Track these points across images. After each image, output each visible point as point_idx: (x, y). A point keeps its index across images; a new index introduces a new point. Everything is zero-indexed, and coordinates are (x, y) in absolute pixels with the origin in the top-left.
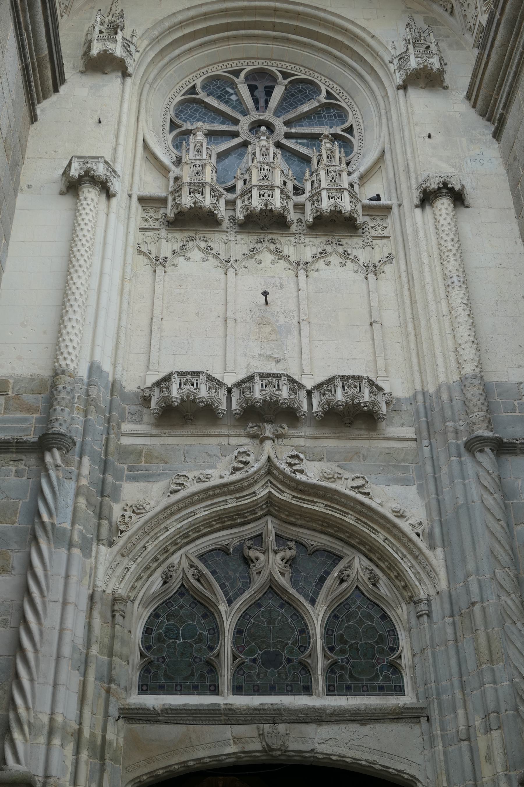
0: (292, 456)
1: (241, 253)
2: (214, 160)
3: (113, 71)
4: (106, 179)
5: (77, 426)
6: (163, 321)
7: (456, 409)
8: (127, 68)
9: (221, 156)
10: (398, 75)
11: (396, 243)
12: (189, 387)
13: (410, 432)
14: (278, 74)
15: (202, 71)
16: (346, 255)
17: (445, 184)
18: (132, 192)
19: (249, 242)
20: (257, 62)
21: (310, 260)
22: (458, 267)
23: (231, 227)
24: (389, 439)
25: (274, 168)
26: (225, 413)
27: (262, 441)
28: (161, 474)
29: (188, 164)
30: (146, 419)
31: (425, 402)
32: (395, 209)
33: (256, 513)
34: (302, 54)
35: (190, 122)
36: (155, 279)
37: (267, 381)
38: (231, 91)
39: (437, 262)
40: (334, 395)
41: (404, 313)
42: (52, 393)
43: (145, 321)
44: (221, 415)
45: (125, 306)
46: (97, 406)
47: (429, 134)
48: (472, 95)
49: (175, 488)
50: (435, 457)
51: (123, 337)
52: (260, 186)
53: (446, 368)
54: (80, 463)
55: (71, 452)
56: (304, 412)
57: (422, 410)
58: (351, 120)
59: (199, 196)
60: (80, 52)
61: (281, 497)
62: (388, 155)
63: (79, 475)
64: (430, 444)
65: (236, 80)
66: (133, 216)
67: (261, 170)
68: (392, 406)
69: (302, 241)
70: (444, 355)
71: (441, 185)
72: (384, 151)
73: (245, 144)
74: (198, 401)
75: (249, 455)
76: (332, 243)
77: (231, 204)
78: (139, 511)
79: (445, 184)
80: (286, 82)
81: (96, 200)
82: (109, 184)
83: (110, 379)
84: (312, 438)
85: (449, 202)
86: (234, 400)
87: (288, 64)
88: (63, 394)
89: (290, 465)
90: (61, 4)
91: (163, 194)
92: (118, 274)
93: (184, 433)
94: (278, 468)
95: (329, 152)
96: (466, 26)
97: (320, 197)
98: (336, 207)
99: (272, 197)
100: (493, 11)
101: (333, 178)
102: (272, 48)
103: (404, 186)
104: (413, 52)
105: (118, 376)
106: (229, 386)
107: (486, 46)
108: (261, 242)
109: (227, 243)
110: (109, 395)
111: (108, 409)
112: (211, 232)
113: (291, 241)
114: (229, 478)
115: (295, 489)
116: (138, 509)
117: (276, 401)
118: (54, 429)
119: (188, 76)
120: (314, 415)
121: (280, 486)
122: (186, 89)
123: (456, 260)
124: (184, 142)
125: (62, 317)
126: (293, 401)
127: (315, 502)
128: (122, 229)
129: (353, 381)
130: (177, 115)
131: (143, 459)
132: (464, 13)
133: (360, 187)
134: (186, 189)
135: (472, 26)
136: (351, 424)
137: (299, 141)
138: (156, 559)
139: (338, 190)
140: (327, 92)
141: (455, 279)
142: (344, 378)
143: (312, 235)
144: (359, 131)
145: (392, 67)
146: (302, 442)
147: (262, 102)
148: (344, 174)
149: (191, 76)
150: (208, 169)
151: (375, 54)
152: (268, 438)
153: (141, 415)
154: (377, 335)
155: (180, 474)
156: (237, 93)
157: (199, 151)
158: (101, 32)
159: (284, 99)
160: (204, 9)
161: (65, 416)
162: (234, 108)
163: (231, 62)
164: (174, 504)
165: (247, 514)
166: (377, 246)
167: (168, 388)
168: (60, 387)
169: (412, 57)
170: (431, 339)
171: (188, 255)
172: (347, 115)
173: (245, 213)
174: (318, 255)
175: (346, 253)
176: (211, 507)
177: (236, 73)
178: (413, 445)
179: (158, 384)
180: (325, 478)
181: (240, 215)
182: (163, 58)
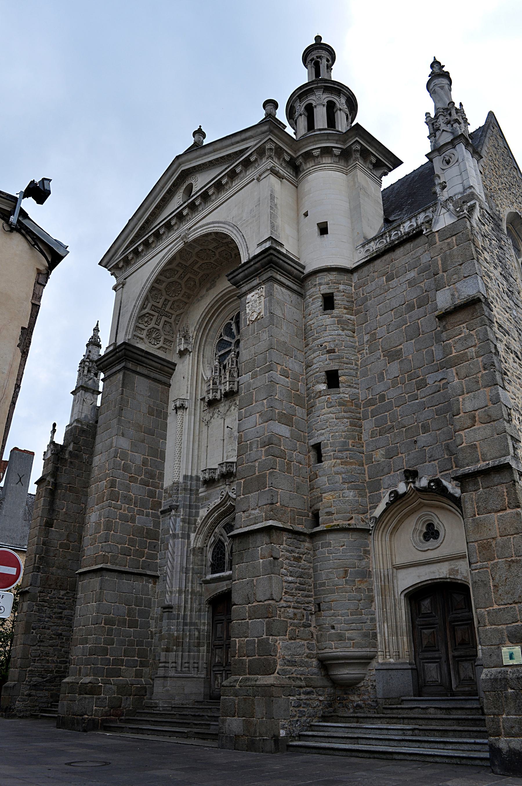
138: (209, 533)
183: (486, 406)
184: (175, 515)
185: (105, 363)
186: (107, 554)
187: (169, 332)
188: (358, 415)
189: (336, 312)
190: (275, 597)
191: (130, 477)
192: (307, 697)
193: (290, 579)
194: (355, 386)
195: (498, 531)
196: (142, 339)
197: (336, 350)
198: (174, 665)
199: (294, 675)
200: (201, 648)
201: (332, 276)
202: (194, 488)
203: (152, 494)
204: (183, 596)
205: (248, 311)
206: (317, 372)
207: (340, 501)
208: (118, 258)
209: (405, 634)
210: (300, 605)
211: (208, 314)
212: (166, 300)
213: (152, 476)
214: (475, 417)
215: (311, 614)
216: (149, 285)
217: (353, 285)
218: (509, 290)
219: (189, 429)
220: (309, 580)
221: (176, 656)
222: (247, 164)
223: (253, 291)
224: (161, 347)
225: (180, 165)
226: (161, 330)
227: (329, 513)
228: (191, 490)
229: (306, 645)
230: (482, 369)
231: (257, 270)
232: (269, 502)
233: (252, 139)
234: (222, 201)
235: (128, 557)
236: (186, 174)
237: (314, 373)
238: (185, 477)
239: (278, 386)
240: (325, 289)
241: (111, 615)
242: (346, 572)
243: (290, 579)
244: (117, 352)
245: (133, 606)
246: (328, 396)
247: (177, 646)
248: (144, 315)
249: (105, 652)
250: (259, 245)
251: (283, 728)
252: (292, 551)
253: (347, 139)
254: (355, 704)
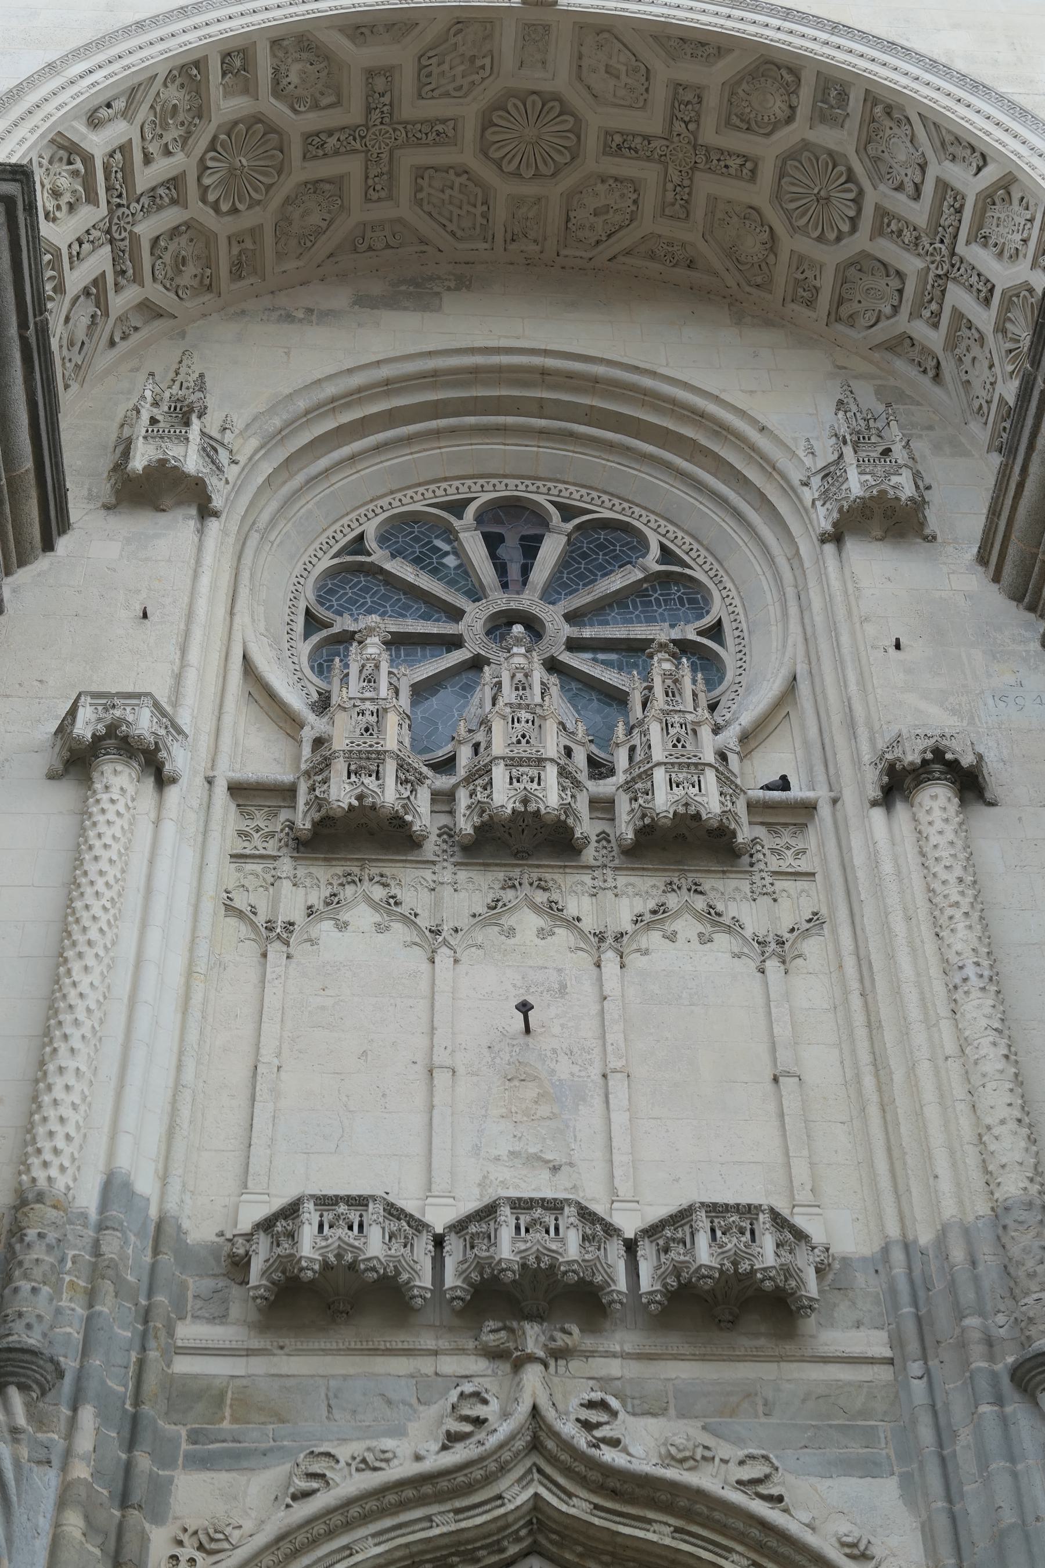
0: (591, 1405)
1: (466, 913)
2: (405, 700)
3: (179, 503)
4: (156, 743)
5: (68, 1330)
6: (282, 1073)
7: (986, 1284)
8: (209, 499)
9: (422, 691)
10: (822, 511)
11: (829, 887)
12: (342, 1232)
13: (876, 1344)
14: (551, 508)
15: (380, 503)
16: (712, 915)
17: (938, 753)
18: (215, 773)
19: (484, 887)
20: (503, 484)
21: (629, 927)
22: (975, 943)
23: (445, 851)
24: (826, 1360)
25: (544, 718)
26: (428, 1295)
27: (518, 1366)
28: (271, 1450)
29: (345, 709)
30: (235, 1311)
31: (910, 1268)
32: (824, 810)
33: (503, 1550)
34: (605, 466)
35: (351, 615)
36: (264, 974)
37: (528, 1218)
38: (446, 547)
39: (926, 932)
40: (691, 1250)
41: (854, 1052)
42: (10, 1247)
43: (237, 1073)
44: (419, 1301)
45: (192, 1036)
46: (118, 1281)
47: (898, 640)
48: (990, 553)
49: (303, 1485)
50: (939, 1405)
51: (185, 1112)
52: (512, 759)
53: (958, 1185)
54: (73, 1423)
55: (50, 1397)
56: (619, 1292)
57: (903, 1286)
58: (717, 609)
59: (370, 782)
60: (106, 463)
61: (564, 1508)
62: (804, 688)
63: (68, 1454)
64: (928, 1373)
65: (456, 523)
66: (215, 826)
67: (513, 723)
68: (831, 1276)
69: (611, 883)
70: (952, 1153)
71: (929, 756)
72: (795, 678)
73: (477, 664)
74: (362, 1266)
75: (485, 1402)
76: (679, 888)
77: (444, 799)
78: (214, 1546)
79: (938, 753)
80: (569, 526)
81: (131, 790)
82: (163, 754)
83: (153, 1212)
84: (639, 1357)
85: (950, 794)
86: (450, 1265)
87: (572, 489)
88: (38, 1252)
89: (588, 1426)
90: (66, 360)
91: (286, 777)
92: (177, 963)
93: (328, 1346)
94: (556, 1435)
95: (669, 682)
96: (970, 405)
97: (649, 783)
98: (687, 805)
99: (539, 784)
100: (1030, 374)
101: (679, 741)
102: (538, 452)
103: (843, 757)
104: (855, 462)
105: (171, 1206)
106: (439, 1230)
107: (1017, 449)
108: (514, 886)
109: (433, 890)
110: (149, 1252)
111: (144, 1287)
112: (398, 865)
113: (583, 883)
114: (437, 1461)
115: (599, 1489)
116: (212, 1540)
117: (552, 1267)
118: (11, 1339)
119: (347, 514)
120: (644, 1300)
121: (561, 1480)
122: (343, 542)
123: (970, 927)
124: (337, 659)
125: (42, 1063)
126: (592, 1266)
127: (650, 1521)
128: (189, 856)
129: (735, 1218)
130: (321, 600)
131: (228, 1412)
132: (965, 378)
133: (741, 760)
134: (339, 767)
135: (985, 405)
136: (732, 1323)
137: (601, 656)
139: (693, 768)
140: (663, 548)
141: (970, 971)
142: (715, 1209)
143: (633, 869)
144: (737, 633)
145: (807, 495)
146: (614, 1368)
147: (514, 571)
148: (705, 732)
149: (354, 515)
150: (392, 720)
151: (769, 467)
152: (531, 1358)
153: (225, 1301)
154: (792, 1104)
155: (317, 1450)
156: (459, 552)
157: (371, 680)
158: (153, 421)
159: (565, 563)
160: (386, 372)
161: (41, 1305)
162: (451, 583)
163: (444, 485)
164: (300, 1527)
165: (481, 1553)
166: (784, 894)
167: (291, 1235)
168: (31, 1234)
169: (853, 474)
170: (919, 1114)
171: (344, 916)
172: (707, 600)
173: (477, 820)
174: (648, 917)
175: (712, 912)
176: (393, 1534)
177: (457, 508)
178: (884, 1374)
179: (267, 1225)
180: (673, 1458)
181: (465, 825)
182: (292, 476)
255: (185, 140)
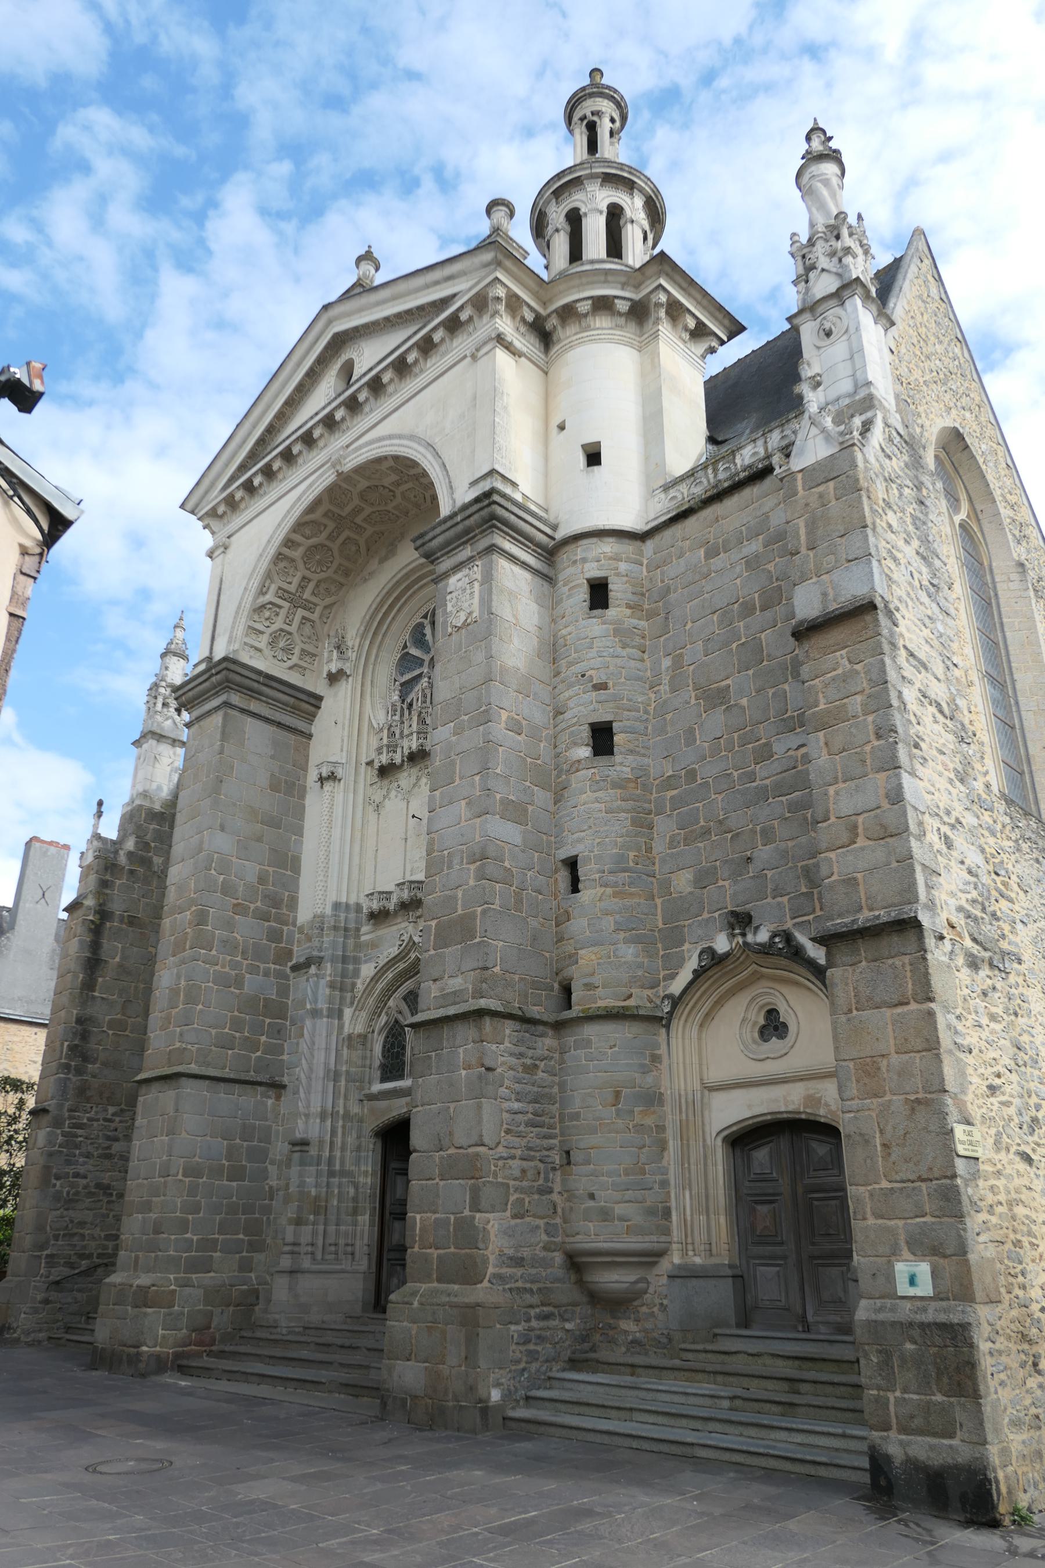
138: (377, 1007)
160: (385, 591)
183: (878, 808)
184: (316, 975)
185: (190, 694)
186: (189, 1047)
187: (309, 638)
188: (646, 805)
189: (611, 613)
190: (486, 1140)
191: (235, 905)
192: (542, 1324)
193: (516, 1106)
194: (643, 751)
195: (892, 1042)
196: (260, 650)
197: (610, 685)
198: (310, 1249)
199: (520, 1284)
200: (359, 1218)
201: (608, 547)
202: (352, 925)
203: (275, 936)
204: (329, 1123)
205: (449, 608)
206: (574, 725)
207: (610, 963)
208: (216, 496)
209: (722, 1211)
210: (532, 1153)
211: (382, 606)
212: (304, 578)
213: (276, 903)
214: (855, 827)
215: (554, 1169)
216: (272, 551)
217: (645, 562)
218: (931, 584)
219: (344, 817)
220: (551, 1107)
221: (314, 1233)
222: (454, 325)
223: (460, 570)
224: (295, 665)
225: (330, 322)
226: (295, 634)
227: (590, 987)
228: (346, 929)
229: (542, 1226)
230: (872, 737)
231: (467, 531)
232: (481, 965)
233: (464, 278)
234: (406, 396)
235: (230, 1052)
236: (340, 342)
237: (569, 727)
238: (337, 906)
239: (501, 749)
240: (594, 571)
241: (197, 1159)
242: (617, 1094)
243: (516, 1106)
244: (212, 675)
245: (238, 1141)
246: (593, 770)
247: (316, 1213)
248: (263, 606)
249: (183, 1226)
250: (474, 483)
251: (498, 1385)
252: (521, 1055)
253: (643, 282)
254: (630, 1338)
255: (296, 568)
